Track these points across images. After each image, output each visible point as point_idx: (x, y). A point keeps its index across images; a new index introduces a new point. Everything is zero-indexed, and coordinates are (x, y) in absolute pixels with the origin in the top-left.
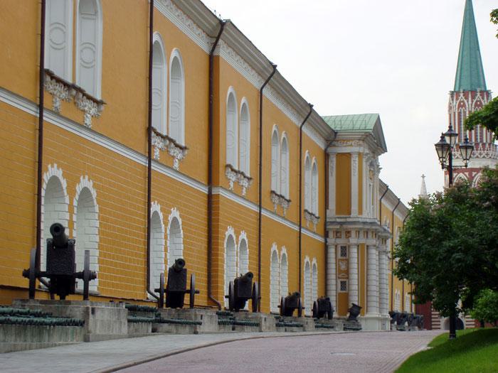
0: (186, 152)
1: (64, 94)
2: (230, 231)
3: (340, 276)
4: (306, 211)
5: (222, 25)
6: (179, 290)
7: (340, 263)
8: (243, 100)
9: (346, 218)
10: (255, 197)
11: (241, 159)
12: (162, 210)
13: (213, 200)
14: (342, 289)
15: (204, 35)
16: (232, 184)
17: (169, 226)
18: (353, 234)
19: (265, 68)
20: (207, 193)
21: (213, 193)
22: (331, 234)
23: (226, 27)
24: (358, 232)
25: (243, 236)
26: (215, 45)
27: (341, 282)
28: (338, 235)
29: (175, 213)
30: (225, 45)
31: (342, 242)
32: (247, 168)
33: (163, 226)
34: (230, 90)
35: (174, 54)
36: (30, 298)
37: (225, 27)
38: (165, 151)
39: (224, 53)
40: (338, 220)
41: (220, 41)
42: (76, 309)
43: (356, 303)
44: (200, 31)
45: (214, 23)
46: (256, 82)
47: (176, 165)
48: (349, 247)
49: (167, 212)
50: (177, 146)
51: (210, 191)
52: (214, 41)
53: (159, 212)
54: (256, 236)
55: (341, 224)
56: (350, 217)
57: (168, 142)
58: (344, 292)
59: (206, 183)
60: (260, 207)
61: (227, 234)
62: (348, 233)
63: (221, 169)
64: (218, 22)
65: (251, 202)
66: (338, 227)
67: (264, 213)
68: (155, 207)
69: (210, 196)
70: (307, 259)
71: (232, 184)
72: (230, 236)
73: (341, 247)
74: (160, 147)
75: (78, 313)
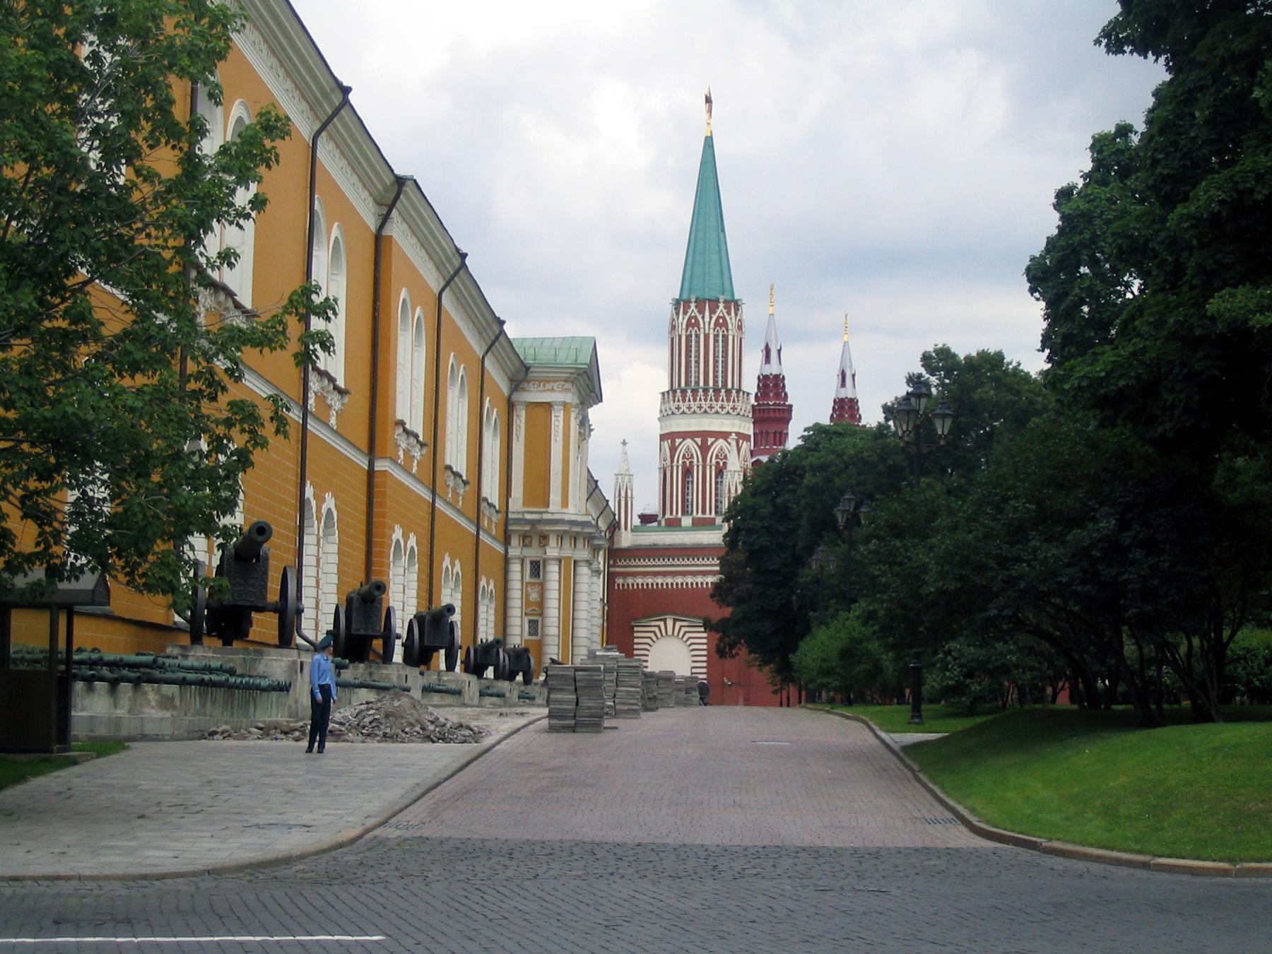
0: (346, 399)
1: (209, 300)
2: (398, 534)
3: (527, 611)
4: (486, 500)
5: (400, 181)
6: (370, 632)
7: (529, 589)
8: (418, 311)
9: (541, 513)
10: (428, 478)
11: (414, 410)
12: (315, 496)
13: (376, 480)
14: (530, 634)
15: (370, 200)
16: (401, 453)
17: (322, 524)
18: (553, 541)
19: (448, 259)
20: (366, 468)
21: (376, 469)
22: (515, 541)
23: (408, 188)
24: (561, 536)
25: (412, 541)
26: (385, 219)
27: (530, 622)
28: (527, 541)
29: (330, 502)
30: (399, 219)
31: (533, 553)
32: (417, 424)
33: (316, 522)
34: (404, 294)
35: (335, 232)
36: (193, 643)
37: (404, 189)
38: (321, 398)
39: (397, 230)
40: (528, 517)
41: (394, 213)
42: (275, 664)
43: (555, 657)
44: (365, 194)
45: (388, 180)
46: (434, 281)
47: (333, 421)
48: (545, 561)
49: (320, 500)
50: (336, 388)
51: (371, 465)
52: (385, 211)
53: (312, 499)
54: (426, 542)
55: (533, 523)
56: (547, 512)
57: (326, 381)
58: (534, 638)
59: (366, 450)
60: (434, 492)
61: (394, 537)
62: (544, 538)
63: (390, 426)
64: (393, 179)
65: (423, 484)
66: (527, 528)
67: (439, 505)
68: (309, 492)
69: (371, 473)
70: (483, 582)
71: (401, 453)
72: (398, 541)
73: (532, 563)
74: (316, 390)
75: (279, 671)
